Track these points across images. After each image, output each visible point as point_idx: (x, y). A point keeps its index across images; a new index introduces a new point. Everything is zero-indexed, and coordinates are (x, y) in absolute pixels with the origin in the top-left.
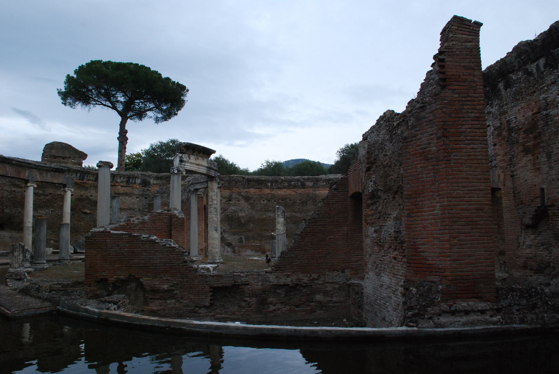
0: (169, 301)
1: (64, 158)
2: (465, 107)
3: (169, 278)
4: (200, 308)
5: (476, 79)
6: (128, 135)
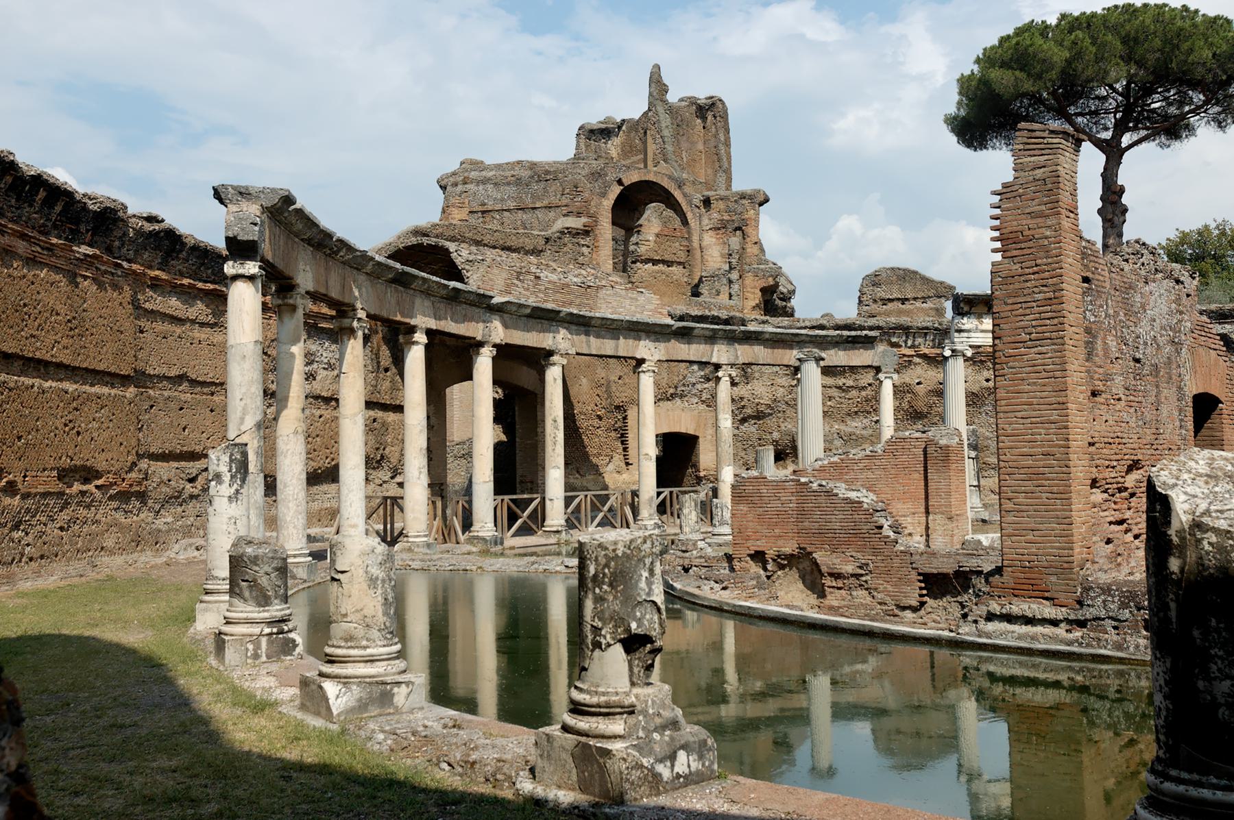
0: (854, 593)
1: (904, 301)
2: (1028, 284)
3: (854, 554)
4: (904, 608)
5: (1048, 233)
6: (1125, 200)
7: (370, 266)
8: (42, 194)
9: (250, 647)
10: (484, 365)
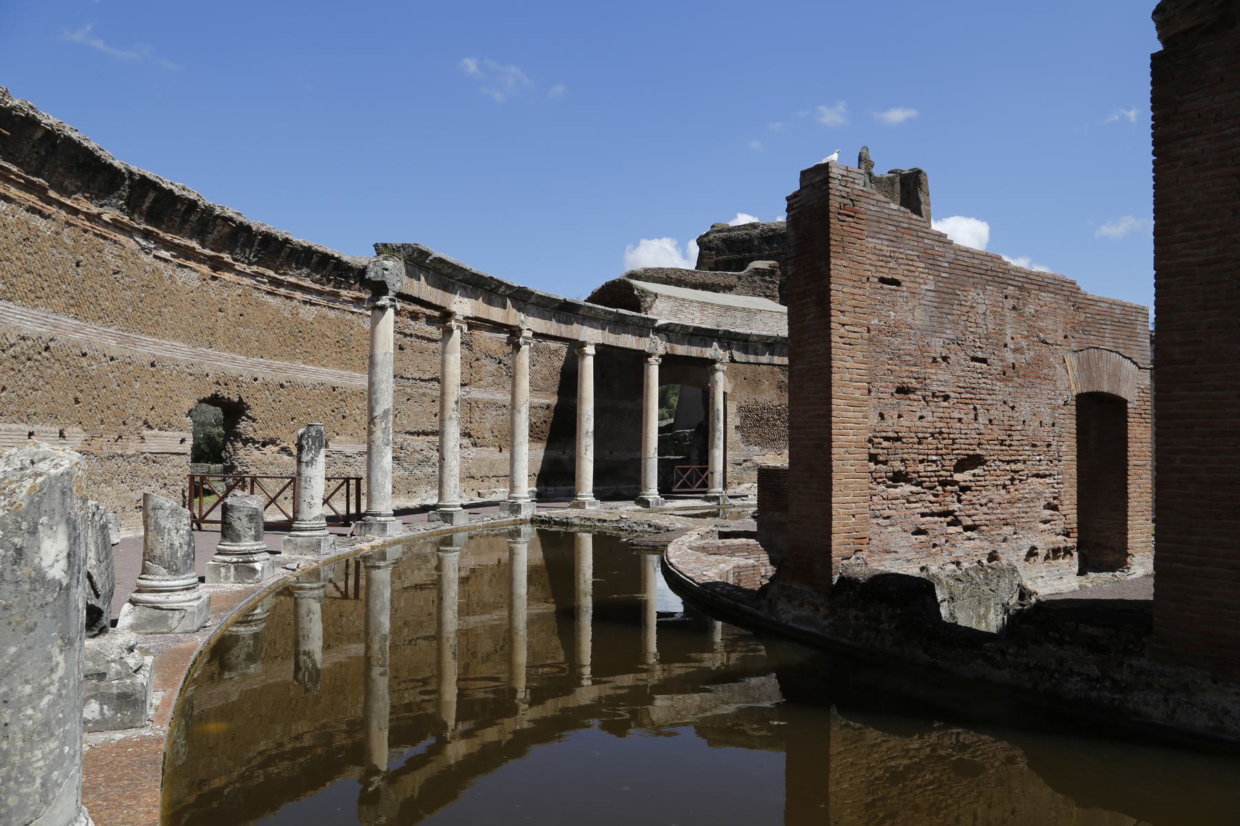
7: (533, 300)
8: (315, 259)
9: (223, 570)
10: (654, 372)
